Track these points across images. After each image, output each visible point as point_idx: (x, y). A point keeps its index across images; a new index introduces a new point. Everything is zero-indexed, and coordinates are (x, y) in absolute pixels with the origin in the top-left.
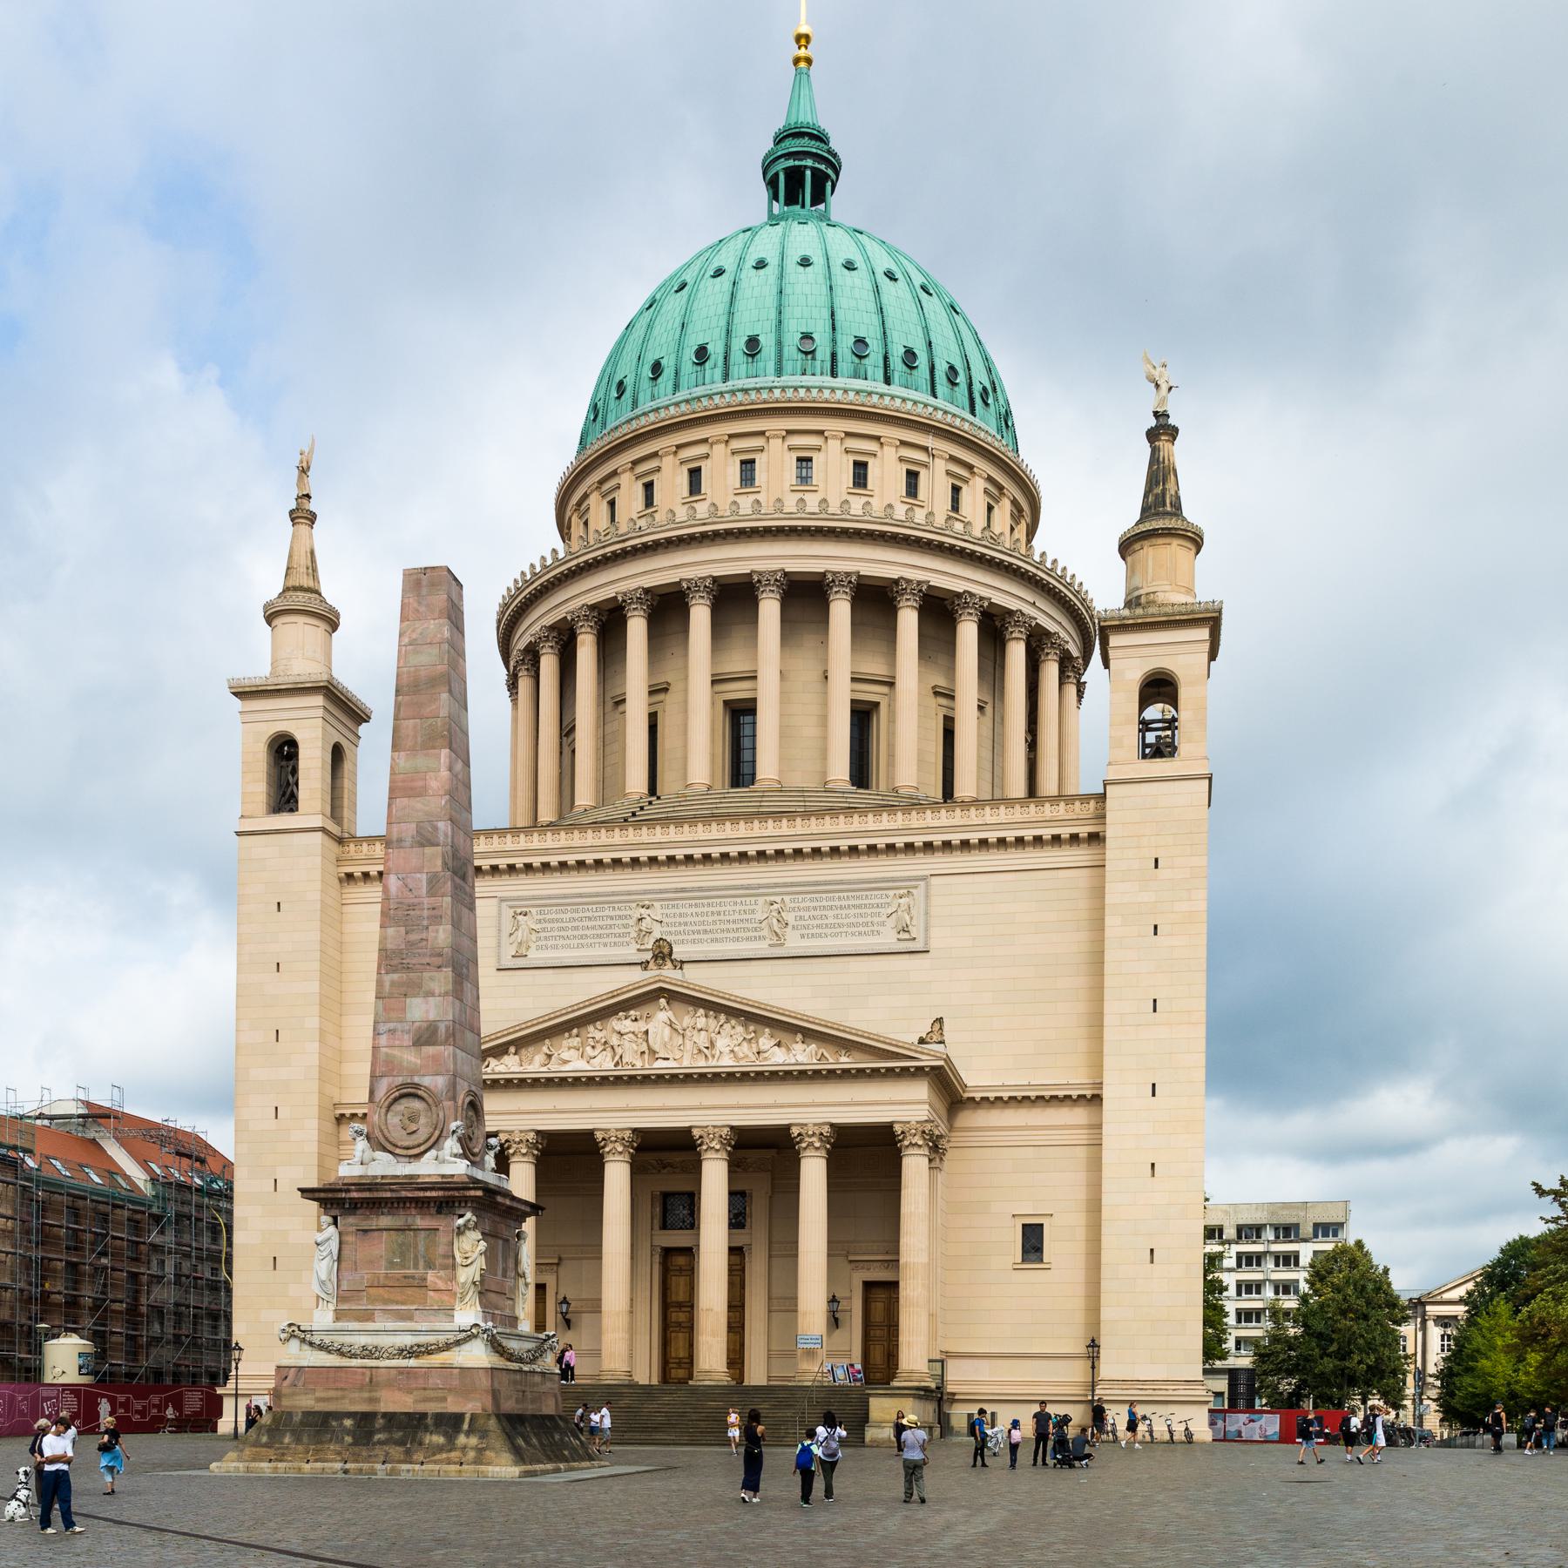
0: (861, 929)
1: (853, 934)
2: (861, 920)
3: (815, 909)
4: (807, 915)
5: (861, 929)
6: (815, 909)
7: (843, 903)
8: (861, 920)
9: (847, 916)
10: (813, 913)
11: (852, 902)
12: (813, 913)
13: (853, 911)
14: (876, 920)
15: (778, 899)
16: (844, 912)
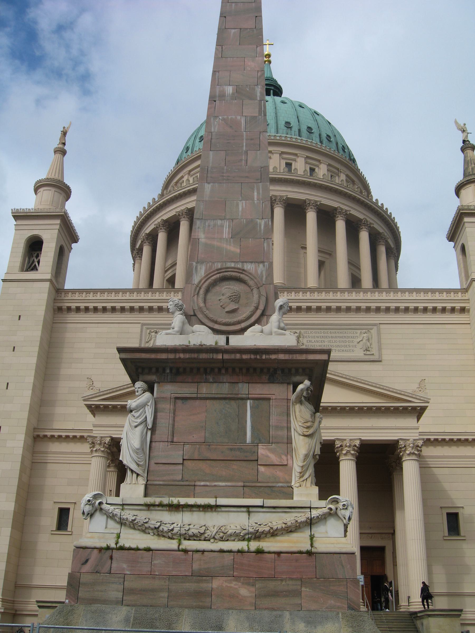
0: (343, 348)
1: (339, 351)
2: (343, 344)
3: (318, 337)
4: (313, 340)
5: (343, 348)
6: (318, 337)
7: (333, 335)
8: (343, 344)
9: (335, 342)
10: (316, 339)
11: (337, 335)
12: (316, 339)
13: (338, 339)
14: (351, 344)
15: (298, 331)
16: (334, 339)
